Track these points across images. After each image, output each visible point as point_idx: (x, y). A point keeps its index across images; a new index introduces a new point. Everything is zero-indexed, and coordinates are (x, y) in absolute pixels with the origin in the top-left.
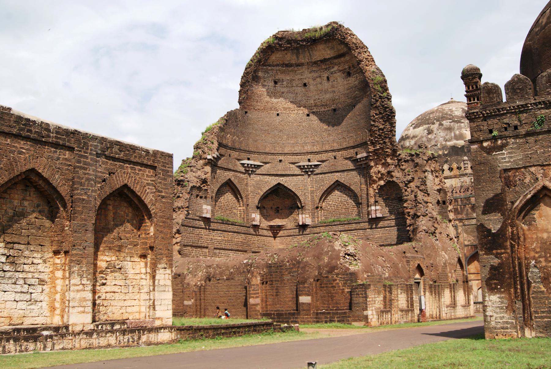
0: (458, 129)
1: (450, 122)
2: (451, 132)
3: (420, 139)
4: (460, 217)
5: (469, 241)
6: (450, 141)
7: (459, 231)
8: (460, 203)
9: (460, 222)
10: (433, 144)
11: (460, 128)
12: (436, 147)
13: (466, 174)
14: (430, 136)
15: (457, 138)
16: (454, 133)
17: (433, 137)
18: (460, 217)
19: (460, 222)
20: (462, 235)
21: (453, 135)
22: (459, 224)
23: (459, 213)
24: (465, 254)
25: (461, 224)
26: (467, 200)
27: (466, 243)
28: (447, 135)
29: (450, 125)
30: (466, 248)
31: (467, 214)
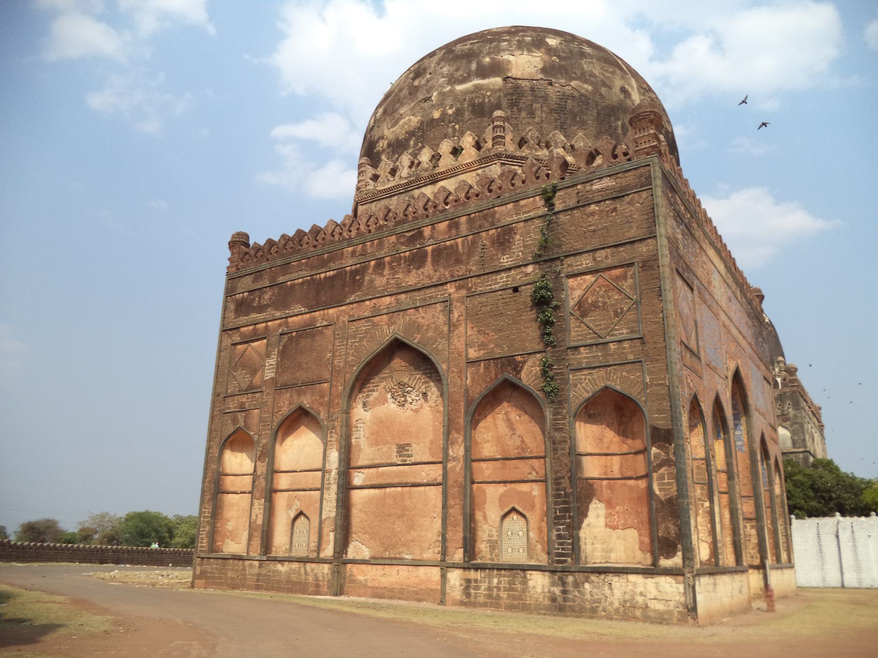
0: (489, 54)
1: (471, 44)
2: (470, 62)
3: (396, 95)
4: (461, 270)
5: (482, 346)
6: (464, 80)
7: (456, 314)
8: (464, 228)
9: (458, 288)
10: (421, 97)
11: (499, 50)
12: (426, 105)
13: (498, 156)
14: (416, 83)
15: (483, 72)
16: (478, 64)
17: (423, 82)
18: (461, 270)
19: (458, 288)
20: (462, 329)
21: (474, 66)
22: (455, 296)
23: (458, 261)
24: (467, 391)
25: (463, 292)
26: (485, 217)
27: (473, 354)
28: (457, 70)
29: (470, 49)
30: (472, 369)
31: (482, 262)
